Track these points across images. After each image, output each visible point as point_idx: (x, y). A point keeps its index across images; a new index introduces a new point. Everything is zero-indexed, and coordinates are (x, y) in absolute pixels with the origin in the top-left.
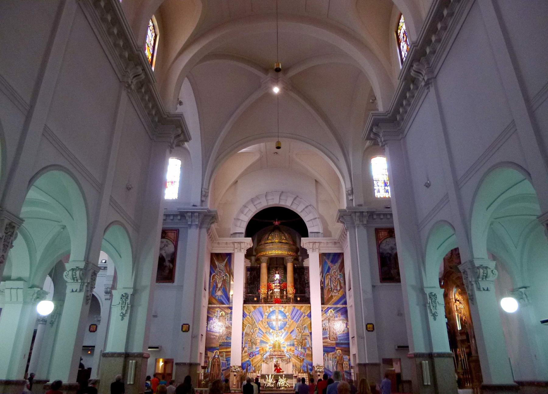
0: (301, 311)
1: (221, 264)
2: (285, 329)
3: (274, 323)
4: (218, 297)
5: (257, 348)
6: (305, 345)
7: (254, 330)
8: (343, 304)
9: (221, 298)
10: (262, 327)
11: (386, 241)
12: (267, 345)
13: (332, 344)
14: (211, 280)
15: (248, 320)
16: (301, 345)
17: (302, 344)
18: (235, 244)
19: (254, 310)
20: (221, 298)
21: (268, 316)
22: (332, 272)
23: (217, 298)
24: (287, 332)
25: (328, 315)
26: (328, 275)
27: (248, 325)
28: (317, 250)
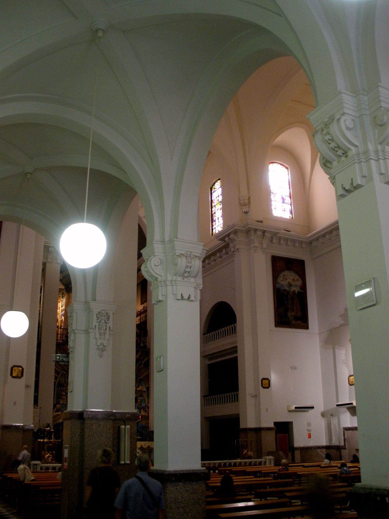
11: (284, 274)
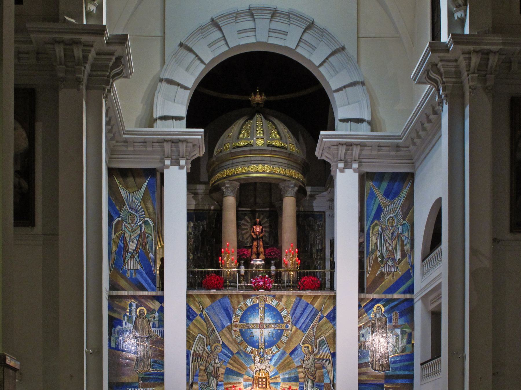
0: (315, 306)
1: (132, 196)
2: (280, 346)
3: (256, 332)
4: (131, 273)
5: (220, 385)
6: (321, 379)
7: (213, 348)
8: (404, 292)
9: (138, 276)
10: (229, 341)
12: (240, 378)
13: (377, 377)
14: (113, 233)
15: (199, 326)
16: (312, 380)
17: (315, 378)
18: (165, 144)
19: (211, 303)
20: (138, 276)
21: (244, 318)
22: (385, 218)
23: (128, 275)
24: (284, 353)
25: (372, 315)
26: (376, 225)
27: (200, 336)
28: (355, 165)
